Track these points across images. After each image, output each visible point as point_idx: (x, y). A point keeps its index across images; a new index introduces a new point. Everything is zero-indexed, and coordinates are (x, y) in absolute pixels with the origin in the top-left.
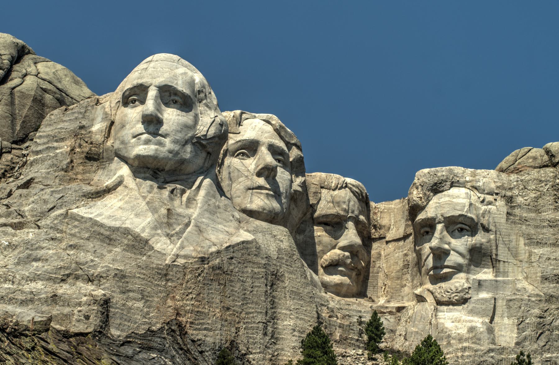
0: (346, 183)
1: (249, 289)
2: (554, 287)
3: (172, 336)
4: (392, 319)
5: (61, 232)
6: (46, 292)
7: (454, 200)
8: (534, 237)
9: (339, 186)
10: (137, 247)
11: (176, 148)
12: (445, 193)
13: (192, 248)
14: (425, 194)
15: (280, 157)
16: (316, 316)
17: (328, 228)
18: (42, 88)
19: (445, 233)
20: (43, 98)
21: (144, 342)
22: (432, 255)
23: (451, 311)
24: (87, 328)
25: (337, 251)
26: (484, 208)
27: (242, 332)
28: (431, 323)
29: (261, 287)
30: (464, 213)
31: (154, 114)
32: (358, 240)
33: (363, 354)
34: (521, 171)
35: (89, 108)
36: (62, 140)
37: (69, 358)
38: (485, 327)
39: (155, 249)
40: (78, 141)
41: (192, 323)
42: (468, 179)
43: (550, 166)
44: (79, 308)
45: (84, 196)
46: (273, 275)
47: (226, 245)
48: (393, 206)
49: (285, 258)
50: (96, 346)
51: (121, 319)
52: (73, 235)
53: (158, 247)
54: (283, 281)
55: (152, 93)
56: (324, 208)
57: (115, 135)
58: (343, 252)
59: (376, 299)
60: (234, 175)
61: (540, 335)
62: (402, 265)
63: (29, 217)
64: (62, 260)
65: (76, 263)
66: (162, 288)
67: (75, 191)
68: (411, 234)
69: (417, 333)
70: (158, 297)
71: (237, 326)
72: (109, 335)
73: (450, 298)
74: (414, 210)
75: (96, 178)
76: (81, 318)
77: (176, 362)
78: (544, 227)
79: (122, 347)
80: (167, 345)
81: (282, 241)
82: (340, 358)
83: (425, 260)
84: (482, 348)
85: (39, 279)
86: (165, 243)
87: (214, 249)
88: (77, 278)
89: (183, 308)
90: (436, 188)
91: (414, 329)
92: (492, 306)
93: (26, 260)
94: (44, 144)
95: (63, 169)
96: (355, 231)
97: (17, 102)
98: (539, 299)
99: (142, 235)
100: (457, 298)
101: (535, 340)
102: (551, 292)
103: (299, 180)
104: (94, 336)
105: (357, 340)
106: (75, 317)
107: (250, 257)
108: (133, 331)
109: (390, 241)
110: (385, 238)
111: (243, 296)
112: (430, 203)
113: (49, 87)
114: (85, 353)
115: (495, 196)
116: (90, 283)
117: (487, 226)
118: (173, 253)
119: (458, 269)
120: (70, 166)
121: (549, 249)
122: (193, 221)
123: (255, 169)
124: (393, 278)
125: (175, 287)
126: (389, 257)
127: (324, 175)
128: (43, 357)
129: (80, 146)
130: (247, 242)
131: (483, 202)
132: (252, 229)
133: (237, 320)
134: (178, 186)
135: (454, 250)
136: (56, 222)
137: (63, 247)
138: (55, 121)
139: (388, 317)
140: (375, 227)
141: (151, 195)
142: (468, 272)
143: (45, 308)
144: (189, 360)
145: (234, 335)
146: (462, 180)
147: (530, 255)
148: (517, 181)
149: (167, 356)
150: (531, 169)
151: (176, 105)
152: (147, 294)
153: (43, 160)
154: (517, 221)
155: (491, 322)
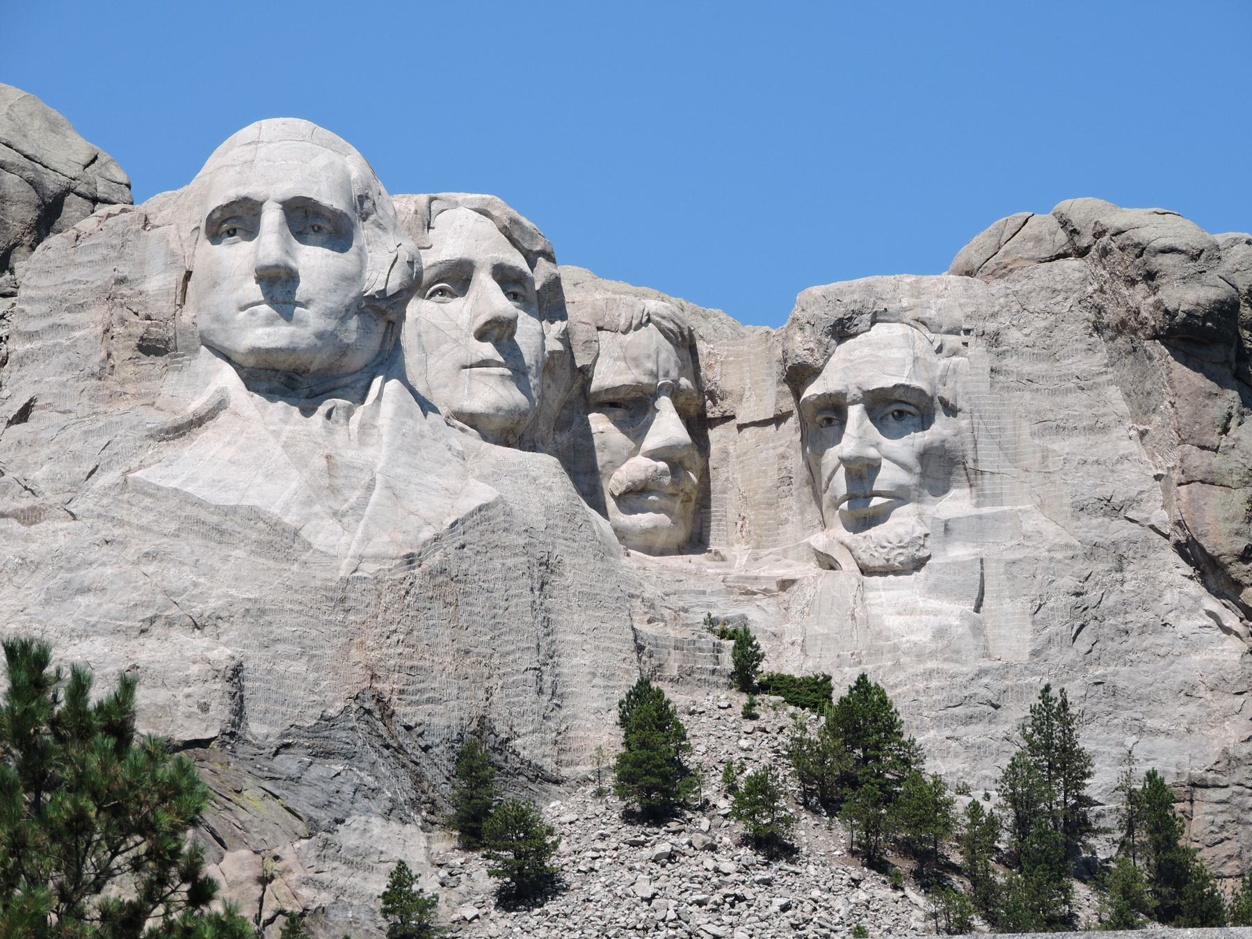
0: (648, 314)
1: (504, 604)
2: (1100, 526)
5: (121, 523)
6: (115, 661)
7: (881, 353)
8: (1050, 416)
9: (635, 322)
10: (278, 546)
13: (386, 538)
14: (820, 342)
15: (516, 290)
16: (631, 637)
17: (619, 413)
19: (868, 422)
21: (318, 742)
22: (842, 470)
26: (943, 362)
28: (853, 617)
33: (730, 706)
34: (1011, 271)
35: (131, 237)
36: (82, 307)
38: (967, 624)
39: (315, 546)
41: (402, 692)
42: (905, 303)
43: (1070, 255)
44: (187, 690)
45: (152, 436)
46: (541, 564)
49: (561, 524)
50: (228, 764)
52: (145, 529)
53: (319, 542)
54: (561, 575)
55: (271, 217)
56: (606, 376)
58: (654, 463)
61: (1078, 631)
62: (776, 477)
63: (48, 494)
64: (135, 588)
66: (338, 629)
67: (132, 428)
68: (790, 414)
71: (487, 685)
72: (249, 737)
73: (888, 560)
75: (166, 392)
76: (192, 709)
77: (379, 774)
78: (1068, 391)
80: (360, 743)
81: (550, 489)
82: (687, 717)
83: (830, 479)
84: (965, 669)
85: (97, 633)
86: (333, 533)
87: (427, 534)
88: (170, 623)
89: (382, 663)
90: (842, 331)
91: (819, 629)
92: (978, 576)
94: (43, 316)
96: (675, 416)
98: (1070, 553)
99: (286, 520)
100: (902, 558)
102: (1093, 536)
104: (223, 744)
105: (714, 672)
107: (495, 537)
108: (292, 722)
110: (733, 417)
111: (492, 621)
116: (197, 632)
117: (951, 402)
118: (351, 552)
119: (899, 496)
120: (108, 367)
122: (379, 477)
123: (472, 321)
124: (759, 503)
126: (750, 460)
129: (123, 321)
131: (939, 350)
133: (486, 671)
134: (340, 402)
135: (887, 458)
136: (105, 501)
137: (131, 559)
138: (58, 264)
140: (712, 395)
141: (288, 427)
144: (404, 766)
145: (482, 704)
146: (893, 307)
149: (362, 765)
151: (320, 238)
152: (311, 643)
153: (47, 354)
154: (1013, 384)
155: (977, 610)
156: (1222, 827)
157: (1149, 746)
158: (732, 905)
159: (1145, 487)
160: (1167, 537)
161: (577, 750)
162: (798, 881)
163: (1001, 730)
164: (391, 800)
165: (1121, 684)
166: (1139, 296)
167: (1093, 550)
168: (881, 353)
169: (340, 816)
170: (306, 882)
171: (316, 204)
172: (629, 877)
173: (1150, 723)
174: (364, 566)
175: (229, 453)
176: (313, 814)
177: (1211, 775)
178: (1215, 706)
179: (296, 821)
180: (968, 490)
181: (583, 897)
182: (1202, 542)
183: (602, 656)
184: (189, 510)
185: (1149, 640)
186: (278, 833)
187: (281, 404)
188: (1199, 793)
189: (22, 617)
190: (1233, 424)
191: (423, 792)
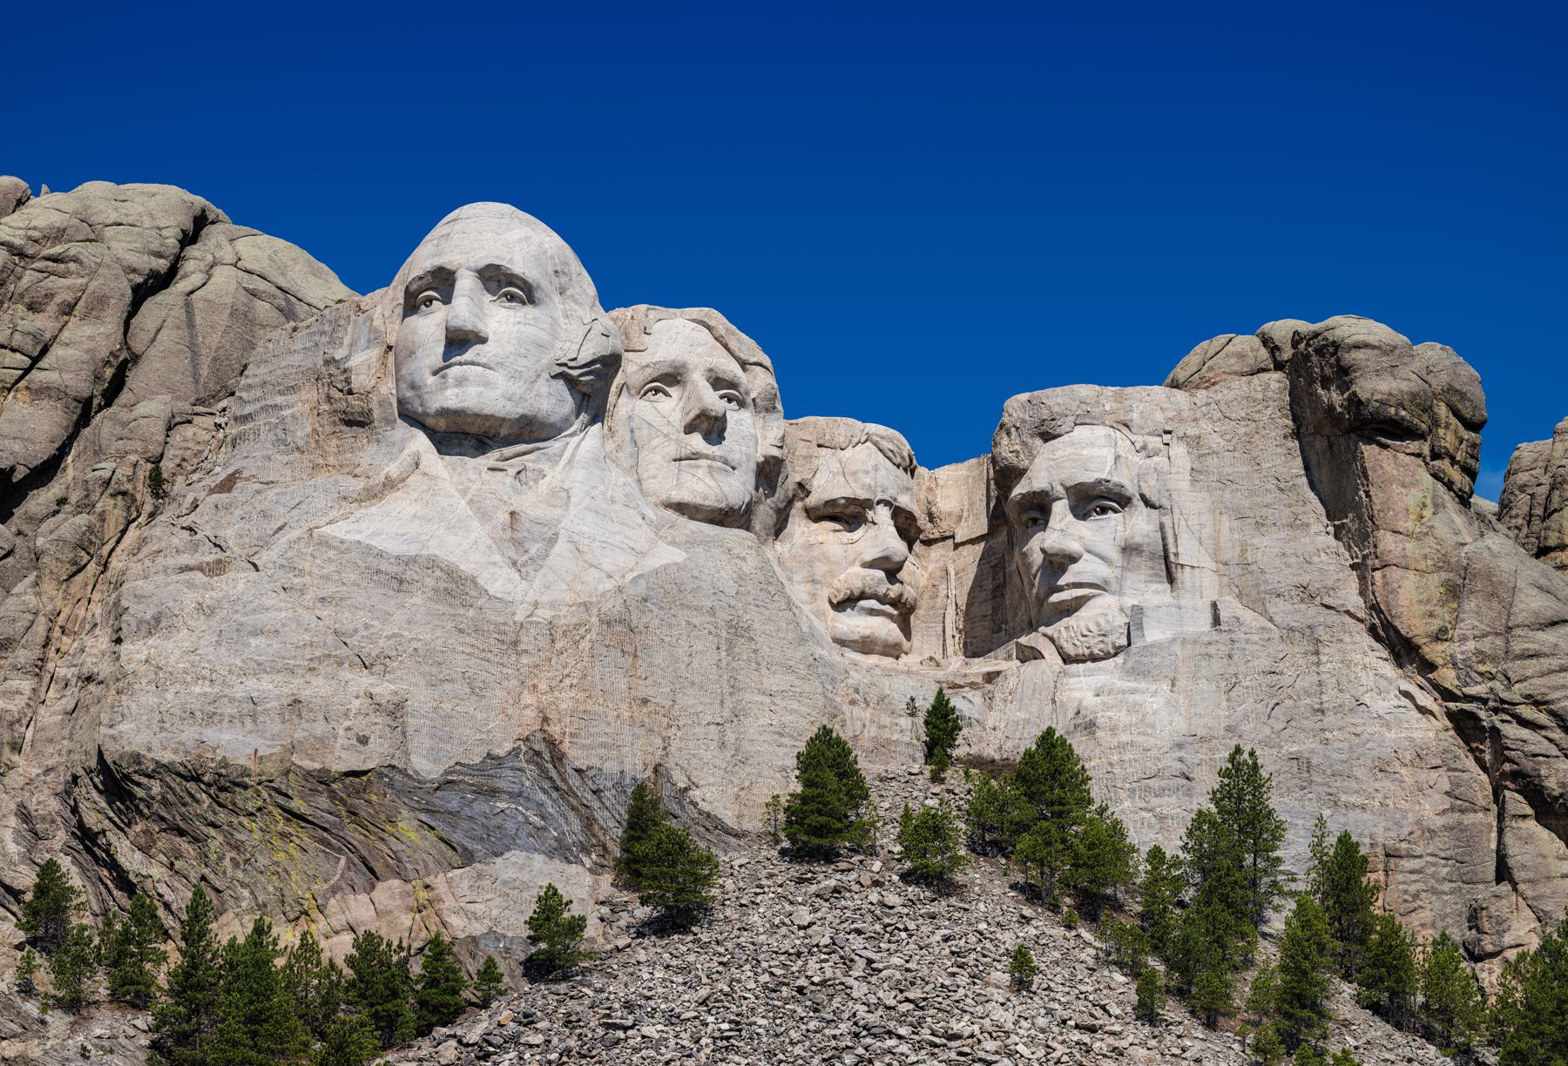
4: (976, 697)
5: (301, 573)
6: (278, 697)
7: (1085, 452)
8: (1249, 513)
9: (855, 440)
11: (517, 388)
12: (1066, 437)
14: (1024, 443)
18: (246, 289)
21: (481, 780)
23: (1091, 673)
25: (857, 569)
27: (675, 744)
28: (1054, 701)
30: (1104, 476)
31: (469, 327)
32: (897, 546)
35: (342, 322)
36: (293, 389)
37: (334, 824)
42: (1108, 408)
47: (631, 576)
51: (433, 736)
52: (327, 578)
53: (495, 589)
55: (466, 283)
59: (942, 662)
60: (641, 435)
66: (510, 671)
69: (1028, 721)
74: (1006, 476)
75: (364, 462)
79: (439, 793)
80: (527, 783)
87: (609, 585)
91: (1021, 715)
96: (893, 529)
97: (198, 320)
98: (1266, 636)
99: (462, 567)
101: (1264, 718)
106: (340, 741)
109: (963, 544)
114: (364, 811)
115: (1167, 438)
119: (1101, 587)
121: (1282, 535)
125: (536, 666)
127: (821, 420)
128: (281, 826)
129: (329, 398)
132: (684, 539)
135: (1089, 552)
139: (970, 695)
145: (660, 752)
146: (1096, 411)
147: (1244, 551)
148: (1208, 404)
156: (1416, 896)
157: (1342, 820)
160: (1361, 621)
164: (556, 839)
168: (1085, 452)
172: (788, 908)
173: (1344, 798)
174: (539, 612)
175: (413, 509)
176: (469, 846)
177: (1404, 845)
179: (450, 853)
182: (1397, 623)
190: (1428, 513)
191: (594, 835)
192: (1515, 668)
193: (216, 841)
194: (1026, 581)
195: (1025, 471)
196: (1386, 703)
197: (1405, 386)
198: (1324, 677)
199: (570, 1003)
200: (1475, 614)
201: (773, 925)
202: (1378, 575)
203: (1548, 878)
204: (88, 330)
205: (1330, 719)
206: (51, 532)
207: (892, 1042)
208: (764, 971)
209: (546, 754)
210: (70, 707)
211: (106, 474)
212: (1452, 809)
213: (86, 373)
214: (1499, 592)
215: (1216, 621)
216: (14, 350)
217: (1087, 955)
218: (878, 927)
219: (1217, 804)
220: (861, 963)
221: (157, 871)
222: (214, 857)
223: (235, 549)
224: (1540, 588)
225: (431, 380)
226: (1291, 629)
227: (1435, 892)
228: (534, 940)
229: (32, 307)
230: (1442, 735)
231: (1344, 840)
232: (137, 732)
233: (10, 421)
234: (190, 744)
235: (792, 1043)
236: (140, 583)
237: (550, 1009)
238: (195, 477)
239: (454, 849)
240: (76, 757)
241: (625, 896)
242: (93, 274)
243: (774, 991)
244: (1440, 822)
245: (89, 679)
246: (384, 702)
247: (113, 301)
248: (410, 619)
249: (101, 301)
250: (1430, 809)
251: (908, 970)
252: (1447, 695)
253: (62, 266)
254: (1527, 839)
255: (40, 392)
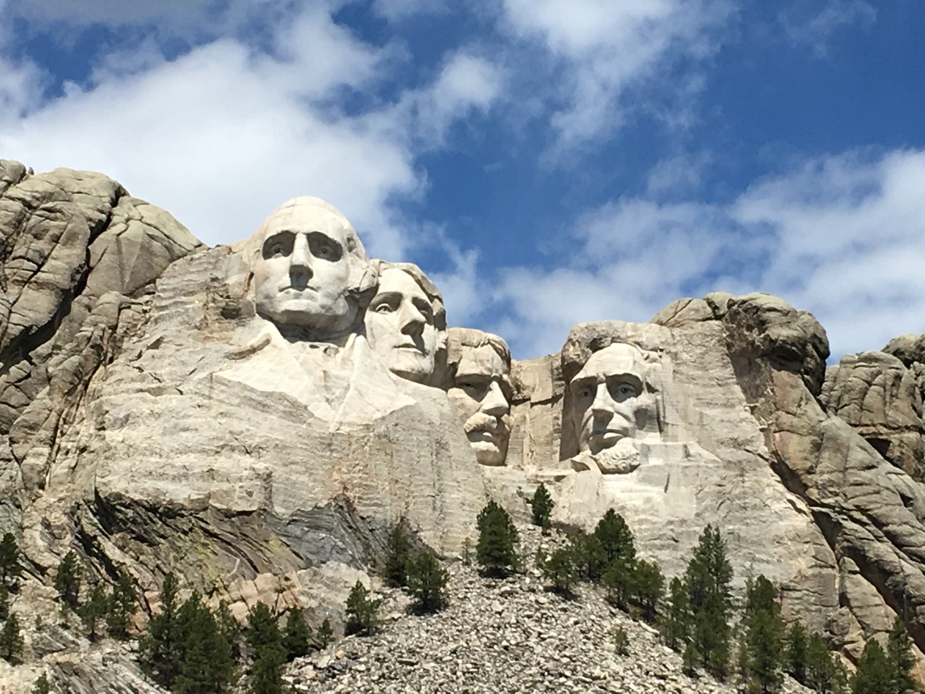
2: (732, 452)
3: (340, 513)
6: (201, 466)
11: (328, 302)
14: (583, 351)
17: (471, 389)
19: (608, 394)
20: (151, 246)
22: (592, 418)
23: (618, 480)
24: (250, 506)
26: (648, 365)
28: (598, 494)
29: (426, 457)
35: (221, 258)
36: (192, 293)
37: (233, 540)
38: (661, 497)
40: (211, 295)
41: (360, 498)
42: (629, 334)
44: (241, 484)
45: (227, 357)
47: (389, 411)
48: (537, 364)
51: (285, 495)
52: (221, 401)
54: (447, 450)
55: (301, 243)
57: (257, 288)
65: (231, 432)
67: (216, 351)
68: (561, 396)
69: (583, 504)
70: (323, 470)
74: (569, 368)
78: (713, 386)
80: (335, 524)
84: (660, 520)
85: (191, 452)
87: (378, 415)
88: (233, 449)
93: (173, 430)
94: (170, 298)
95: (196, 327)
97: (124, 250)
99: (300, 400)
103: (443, 335)
105: (524, 514)
106: (237, 493)
109: (536, 404)
110: (529, 399)
112: (590, 360)
113: (157, 233)
115: (660, 353)
119: (625, 433)
121: (720, 410)
125: (341, 458)
129: (214, 300)
130: (410, 406)
134: (332, 345)
135: (618, 413)
136: (199, 386)
142: (633, 436)
143: (200, 484)
144: (359, 539)
145: (404, 510)
146: (622, 336)
150: (694, 322)
153: (171, 317)
156: (798, 612)
158: (547, 619)
159: (755, 434)
160: (767, 460)
161: (452, 543)
162: (582, 612)
163: (679, 554)
164: (351, 555)
165: (742, 535)
166: (755, 336)
167: (728, 464)
169: (324, 560)
170: (303, 594)
171: (325, 237)
172: (488, 602)
173: (757, 556)
176: (310, 556)
177: (793, 584)
178: (793, 548)
179: (299, 560)
180: (658, 433)
181: (461, 610)
182: (787, 462)
183: (468, 495)
184: (247, 393)
185: (757, 513)
186: (288, 565)
187: (300, 343)
188: (785, 593)
189: (149, 441)
190: (803, 403)
191: (370, 555)
192: (849, 490)
193: (164, 544)
194: (577, 426)
195: (583, 366)
196: (780, 506)
197: (795, 333)
198: (747, 490)
199: (376, 648)
200: (827, 461)
201: (480, 610)
202: (777, 435)
203: (869, 606)
204: (66, 252)
205: (749, 513)
206: (58, 365)
207: (562, 680)
208: (483, 636)
209: (345, 507)
210: (73, 465)
211: (89, 334)
212: (816, 566)
213: (67, 276)
214: (840, 448)
215: (688, 455)
216: (29, 260)
217: (649, 636)
218: (538, 614)
219: (697, 556)
220: (535, 634)
221: (128, 561)
222: (163, 554)
223: (168, 383)
224: (861, 448)
225: (280, 294)
226: (730, 462)
227: (807, 610)
228: (348, 612)
229: (37, 237)
230: (811, 525)
231: (761, 578)
232: (117, 481)
233: (26, 300)
234: (150, 490)
235: (508, 677)
236: (113, 397)
237: (365, 651)
238: (135, 339)
239: (301, 558)
240: (79, 493)
241: (388, 591)
242: (69, 220)
243: (490, 647)
244: (810, 572)
245: (83, 450)
246: (261, 473)
247: (80, 237)
248: (267, 427)
249: (72, 237)
250: (803, 564)
251: (560, 640)
252: (811, 503)
253: (53, 215)
254: (857, 584)
255: (41, 285)
